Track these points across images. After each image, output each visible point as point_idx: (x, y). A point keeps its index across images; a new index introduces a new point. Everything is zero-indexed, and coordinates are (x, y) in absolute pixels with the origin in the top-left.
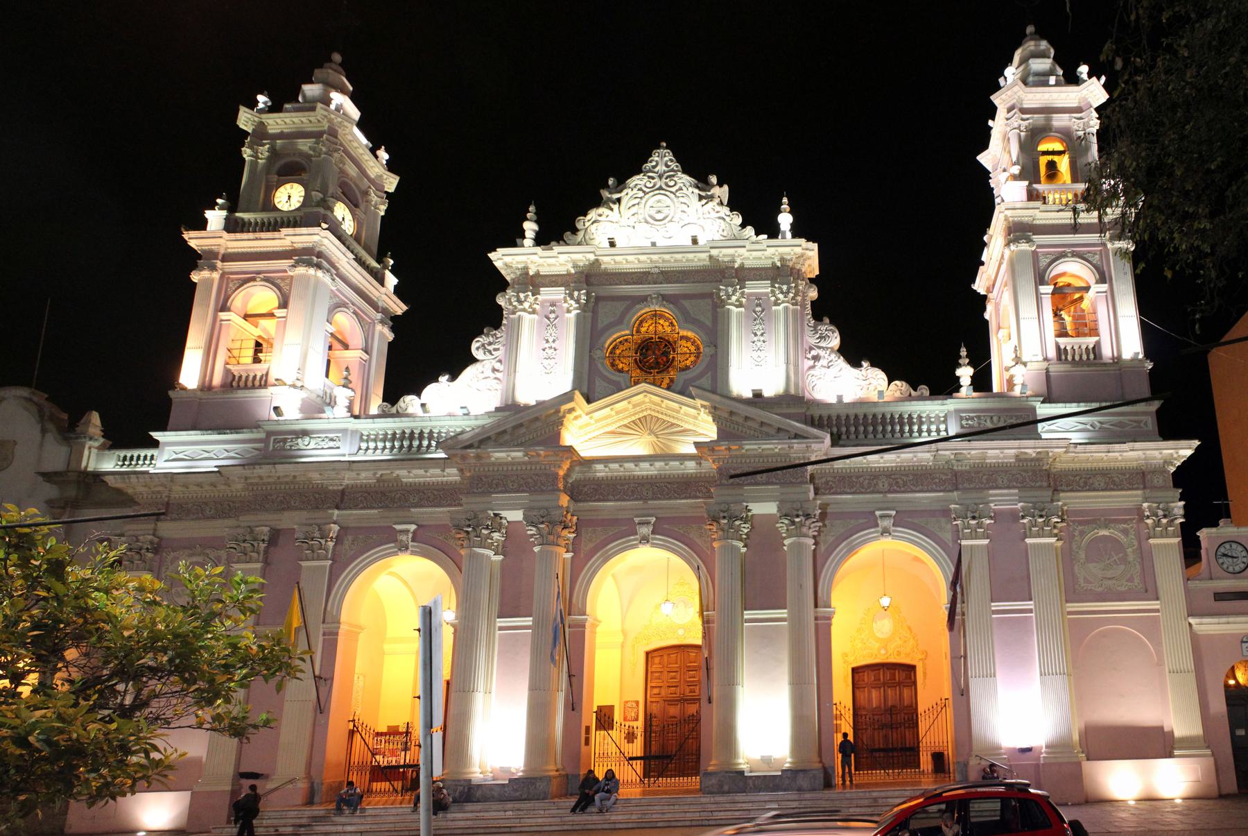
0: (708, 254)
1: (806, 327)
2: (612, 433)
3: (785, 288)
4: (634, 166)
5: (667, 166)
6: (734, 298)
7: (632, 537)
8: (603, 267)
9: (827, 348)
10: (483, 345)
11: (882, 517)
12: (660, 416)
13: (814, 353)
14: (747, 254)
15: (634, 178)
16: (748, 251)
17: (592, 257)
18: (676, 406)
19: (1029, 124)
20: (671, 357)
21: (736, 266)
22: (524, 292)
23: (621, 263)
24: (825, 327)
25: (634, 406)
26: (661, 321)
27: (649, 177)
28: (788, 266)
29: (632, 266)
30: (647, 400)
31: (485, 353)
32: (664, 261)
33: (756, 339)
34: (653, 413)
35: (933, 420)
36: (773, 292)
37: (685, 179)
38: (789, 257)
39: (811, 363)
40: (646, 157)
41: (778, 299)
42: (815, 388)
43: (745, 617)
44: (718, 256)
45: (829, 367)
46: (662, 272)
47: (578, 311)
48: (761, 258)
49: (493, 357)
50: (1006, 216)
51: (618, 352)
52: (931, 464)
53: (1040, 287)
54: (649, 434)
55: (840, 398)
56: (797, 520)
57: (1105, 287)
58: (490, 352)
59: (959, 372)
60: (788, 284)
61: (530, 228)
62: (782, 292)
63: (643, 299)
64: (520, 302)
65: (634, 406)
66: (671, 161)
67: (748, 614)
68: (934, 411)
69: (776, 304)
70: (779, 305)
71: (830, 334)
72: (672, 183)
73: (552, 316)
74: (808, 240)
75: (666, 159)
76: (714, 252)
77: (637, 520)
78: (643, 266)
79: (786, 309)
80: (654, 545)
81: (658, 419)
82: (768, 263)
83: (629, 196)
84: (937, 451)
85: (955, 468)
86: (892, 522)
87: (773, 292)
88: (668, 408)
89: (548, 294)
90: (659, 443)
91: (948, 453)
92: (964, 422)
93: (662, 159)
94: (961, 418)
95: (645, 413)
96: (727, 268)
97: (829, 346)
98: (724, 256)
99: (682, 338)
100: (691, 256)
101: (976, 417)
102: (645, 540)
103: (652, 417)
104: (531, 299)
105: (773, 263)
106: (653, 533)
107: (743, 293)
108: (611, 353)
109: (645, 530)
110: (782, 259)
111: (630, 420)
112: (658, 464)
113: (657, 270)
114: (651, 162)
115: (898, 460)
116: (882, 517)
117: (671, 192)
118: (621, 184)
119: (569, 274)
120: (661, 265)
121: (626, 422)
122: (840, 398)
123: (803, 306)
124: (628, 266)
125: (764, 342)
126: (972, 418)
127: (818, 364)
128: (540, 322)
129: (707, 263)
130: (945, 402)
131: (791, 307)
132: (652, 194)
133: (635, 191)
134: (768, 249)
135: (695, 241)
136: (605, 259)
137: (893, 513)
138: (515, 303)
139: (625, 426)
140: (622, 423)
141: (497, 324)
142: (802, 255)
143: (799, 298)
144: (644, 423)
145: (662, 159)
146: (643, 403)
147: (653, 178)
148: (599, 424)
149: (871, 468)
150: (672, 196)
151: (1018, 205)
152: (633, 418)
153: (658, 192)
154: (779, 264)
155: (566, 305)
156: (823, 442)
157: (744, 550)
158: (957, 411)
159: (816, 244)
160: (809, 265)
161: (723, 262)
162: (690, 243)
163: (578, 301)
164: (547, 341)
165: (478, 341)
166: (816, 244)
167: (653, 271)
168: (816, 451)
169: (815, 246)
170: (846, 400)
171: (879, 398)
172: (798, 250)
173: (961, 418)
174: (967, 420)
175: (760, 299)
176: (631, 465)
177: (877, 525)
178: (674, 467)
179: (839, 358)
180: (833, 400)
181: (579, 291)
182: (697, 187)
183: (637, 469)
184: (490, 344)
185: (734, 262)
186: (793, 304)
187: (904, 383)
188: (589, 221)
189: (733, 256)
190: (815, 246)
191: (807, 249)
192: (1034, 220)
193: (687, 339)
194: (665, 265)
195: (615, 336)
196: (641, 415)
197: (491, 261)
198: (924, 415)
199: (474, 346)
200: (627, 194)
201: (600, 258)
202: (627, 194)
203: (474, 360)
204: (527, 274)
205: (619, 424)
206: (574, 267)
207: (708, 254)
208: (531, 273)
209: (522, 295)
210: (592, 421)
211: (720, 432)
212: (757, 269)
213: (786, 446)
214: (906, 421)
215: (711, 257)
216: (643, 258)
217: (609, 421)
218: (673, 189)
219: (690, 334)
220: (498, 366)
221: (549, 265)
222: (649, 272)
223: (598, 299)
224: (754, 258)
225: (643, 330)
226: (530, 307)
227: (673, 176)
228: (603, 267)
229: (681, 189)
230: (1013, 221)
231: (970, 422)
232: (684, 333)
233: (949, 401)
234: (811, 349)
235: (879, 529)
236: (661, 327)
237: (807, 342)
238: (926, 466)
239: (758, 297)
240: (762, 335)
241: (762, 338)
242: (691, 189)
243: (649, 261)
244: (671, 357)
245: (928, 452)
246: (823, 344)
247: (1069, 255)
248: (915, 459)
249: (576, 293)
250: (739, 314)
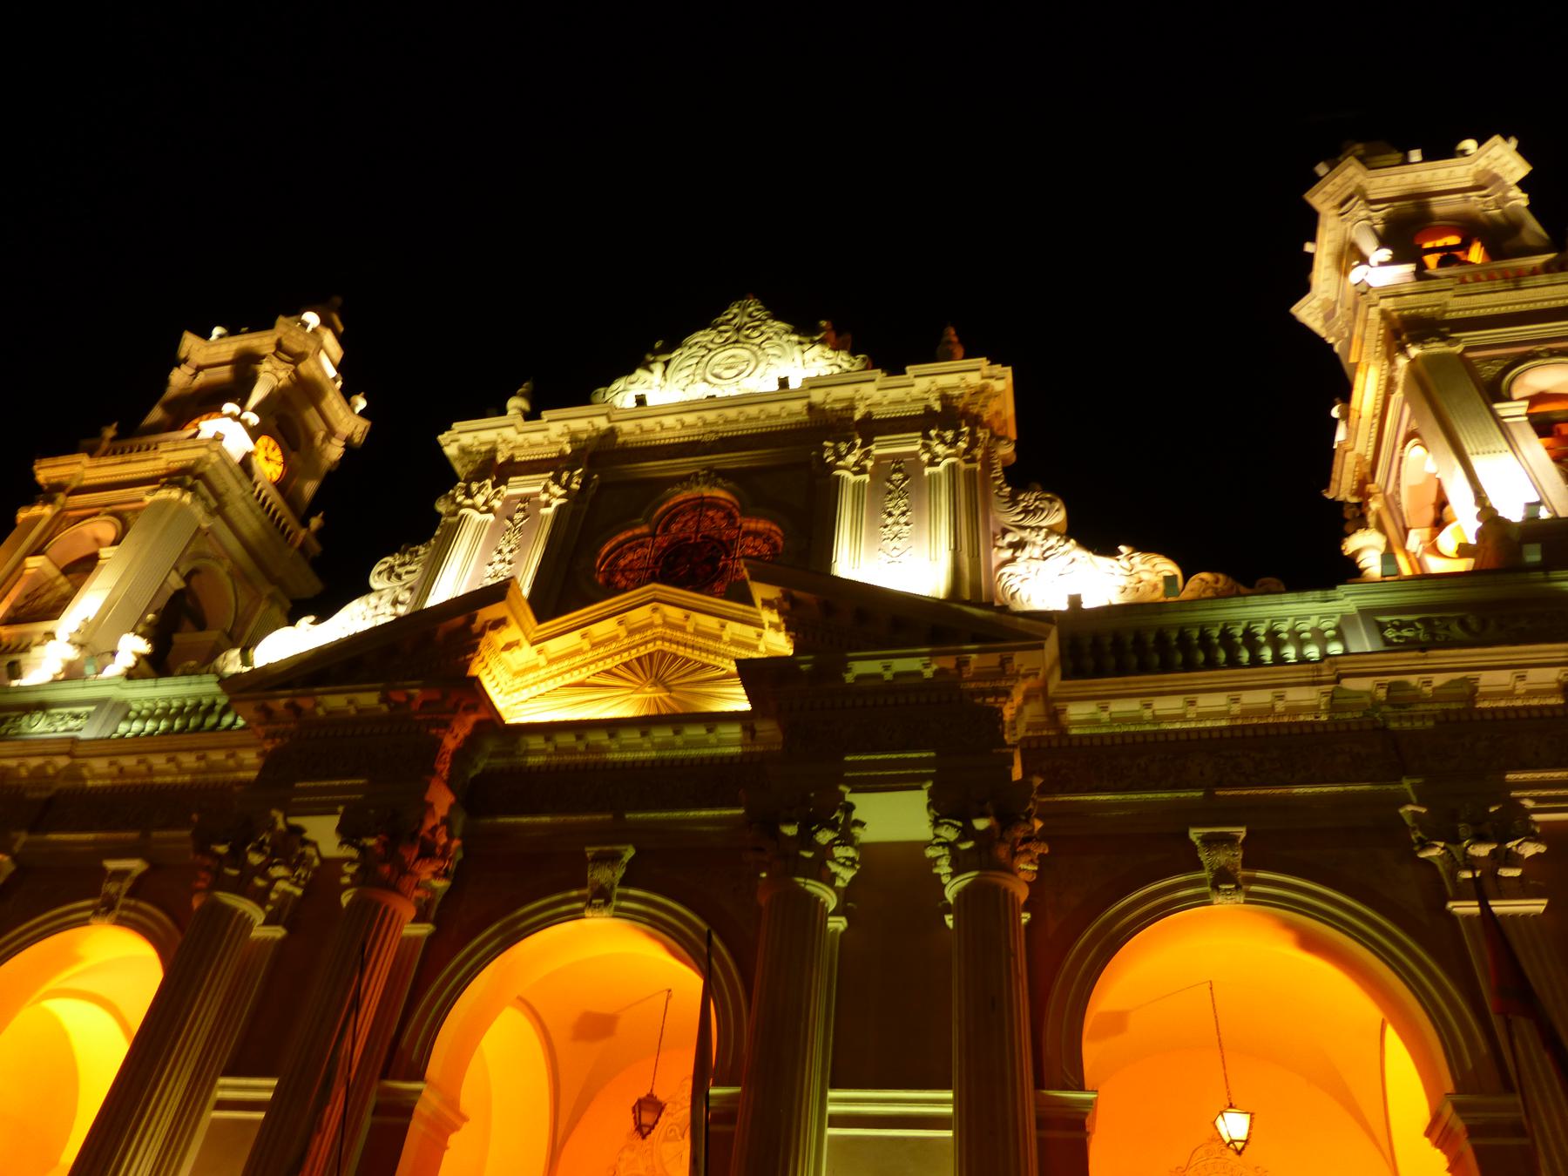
0: (805, 401)
1: (994, 499)
2: (581, 684)
3: (949, 435)
5: (750, 315)
6: (851, 459)
7: (574, 893)
8: (620, 440)
9: (1040, 528)
10: (391, 568)
11: (1210, 841)
12: (681, 651)
13: (1010, 538)
14: (877, 396)
15: (695, 335)
16: (879, 389)
17: (602, 423)
18: (710, 623)
19: (1388, 214)
20: (721, 564)
21: (858, 416)
22: (479, 481)
23: (652, 431)
24: (1027, 499)
25: (631, 633)
26: (711, 513)
27: (720, 332)
28: (957, 407)
29: (671, 434)
30: (657, 619)
31: (389, 579)
32: (726, 422)
33: (890, 521)
34: (667, 647)
35: (1307, 635)
36: (927, 448)
38: (956, 393)
39: (1008, 554)
41: (935, 456)
42: (1017, 595)
43: (832, 1109)
44: (824, 402)
45: (1045, 559)
46: (722, 439)
47: (563, 501)
48: (902, 402)
49: (402, 583)
50: (1384, 314)
51: (622, 563)
52: (1324, 718)
53: (1497, 406)
54: (654, 684)
55: (1075, 601)
56: (981, 824)
58: (399, 577)
59: (1351, 544)
60: (956, 428)
62: (943, 442)
64: (469, 495)
65: (631, 633)
66: (758, 310)
67: (841, 1101)
68: (1307, 617)
69: (932, 463)
70: (938, 464)
71: (1045, 504)
72: (755, 334)
73: (519, 516)
74: (993, 362)
75: (750, 309)
76: (817, 396)
77: (590, 851)
78: (689, 432)
79: (952, 468)
80: (621, 913)
81: (676, 657)
82: (918, 409)
83: (683, 356)
84: (1337, 681)
85: (1394, 725)
86: (1240, 854)
87: (924, 446)
88: (698, 633)
89: (518, 487)
90: (667, 700)
91: (1365, 684)
92: (1390, 634)
94: (1382, 627)
95: (651, 648)
96: (840, 419)
97: (1043, 524)
98: (835, 401)
99: (747, 533)
100: (774, 408)
101: (1419, 620)
102: (602, 897)
103: (664, 654)
104: (489, 491)
105: (928, 409)
106: (624, 882)
107: (867, 455)
108: (609, 565)
109: (603, 875)
110: (945, 397)
111: (618, 660)
112: (662, 734)
113: (713, 437)
114: (726, 314)
115: (1236, 709)
116: (1208, 841)
117: (753, 344)
119: (562, 456)
120: (721, 428)
121: (609, 664)
122: (1075, 601)
123: (988, 465)
124: (664, 435)
125: (907, 524)
126: (1410, 625)
127: (1022, 555)
128: (494, 527)
129: (804, 417)
130: (1331, 593)
131: (963, 466)
132: (719, 350)
133: (695, 349)
134: (918, 381)
135: (783, 383)
136: (627, 426)
137: (1241, 832)
138: (460, 499)
139: (608, 672)
140: (601, 666)
141: (423, 536)
142: (983, 389)
143: (979, 453)
144: (652, 668)
146: (651, 626)
147: (726, 331)
148: (554, 668)
149: (1167, 733)
150: (756, 348)
151: (1406, 290)
152: (626, 657)
153: (731, 346)
154: (937, 407)
155: (544, 497)
156: (1041, 647)
157: (838, 924)
158: (1367, 614)
159: (1009, 369)
160: (998, 413)
161: (833, 410)
162: (775, 387)
163: (566, 486)
164: (500, 552)
165: (386, 563)
166: (1009, 369)
167: (706, 438)
168: (1026, 676)
169: (1008, 372)
170: (1088, 603)
171: (1166, 594)
172: (974, 379)
173: (1382, 627)
174: (1398, 628)
175: (901, 462)
176: (601, 738)
177: (1199, 866)
178: (694, 743)
179: (1067, 541)
180: (1063, 606)
181: (572, 470)
182: (794, 332)
183: (615, 746)
184: (403, 565)
185: (852, 408)
186: (967, 461)
187: (1221, 577)
188: (612, 392)
189: (852, 399)
190: (1008, 372)
191: (991, 377)
192: (1445, 312)
193: (756, 534)
194: (729, 427)
195: (622, 537)
196: (643, 651)
197: (439, 448)
198: (1285, 627)
199: (378, 568)
200: (681, 354)
201: (618, 424)
202: (681, 354)
203: (369, 590)
204: (494, 459)
205: (593, 669)
206: (571, 442)
207: (805, 401)
208: (500, 459)
209: (474, 486)
210: (542, 660)
211: (796, 648)
212: (895, 419)
213: (949, 663)
214: (1240, 640)
215: (811, 408)
216: (690, 419)
217: (578, 660)
218: (758, 341)
219: (761, 525)
221: (532, 446)
222: (698, 442)
223: (602, 487)
224: (891, 403)
225: (674, 528)
226: (486, 503)
227: (760, 326)
228: (620, 440)
229: (768, 339)
230: (1401, 317)
231: (1405, 633)
233: (1342, 589)
234: (1005, 532)
235: (1205, 874)
236: (708, 522)
237: (996, 521)
238: (1311, 724)
239: (897, 458)
240: (903, 514)
241: (903, 520)
242: (785, 337)
243: (700, 424)
244: (721, 564)
245: (1314, 684)
246: (1031, 522)
247: (1545, 355)
248: (1280, 706)
249: (565, 476)
250: (858, 487)
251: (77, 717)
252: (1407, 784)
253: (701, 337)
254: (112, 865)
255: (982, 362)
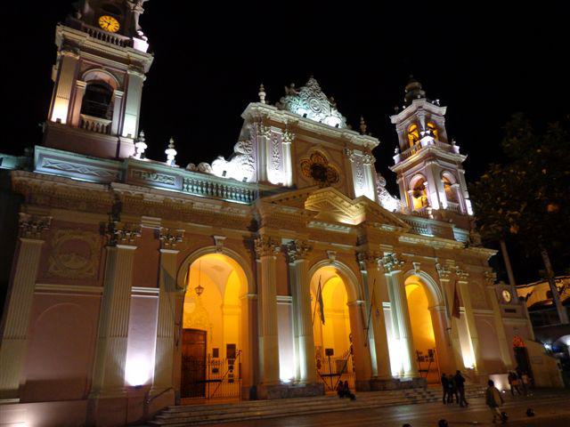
4: (301, 83)
37: (324, 96)
40: (307, 81)
57: (458, 185)
61: (263, 95)
63: (314, 145)
82: (361, 144)
93: (313, 82)
109: (333, 257)
118: (298, 88)
119: (283, 123)
145: (313, 82)
215: (342, 136)
220: (251, 159)
232: (330, 165)
251: (169, 179)
252: (436, 259)
253: (305, 89)
254: (216, 237)
255: (377, 139)
